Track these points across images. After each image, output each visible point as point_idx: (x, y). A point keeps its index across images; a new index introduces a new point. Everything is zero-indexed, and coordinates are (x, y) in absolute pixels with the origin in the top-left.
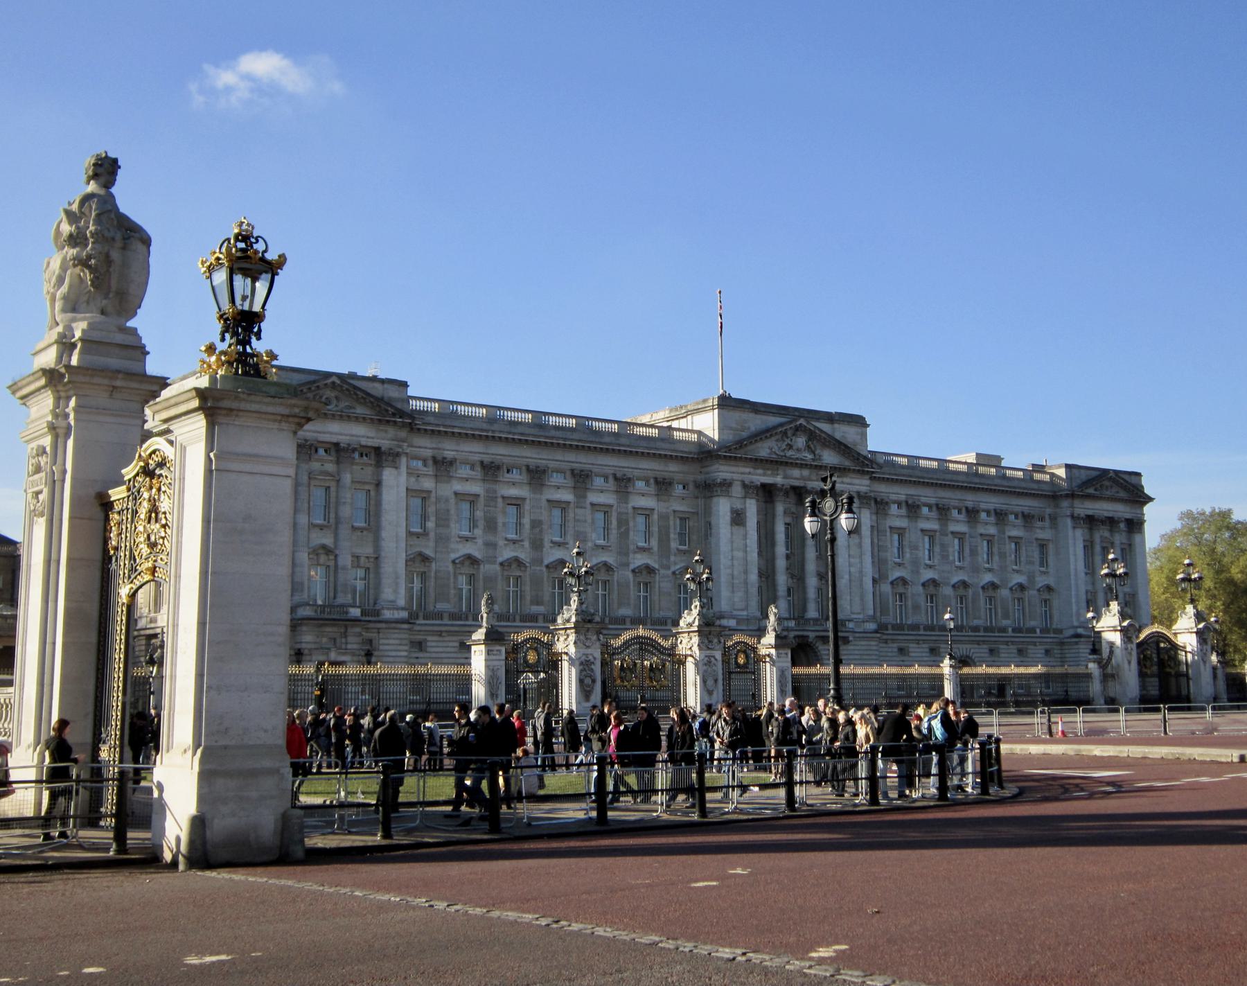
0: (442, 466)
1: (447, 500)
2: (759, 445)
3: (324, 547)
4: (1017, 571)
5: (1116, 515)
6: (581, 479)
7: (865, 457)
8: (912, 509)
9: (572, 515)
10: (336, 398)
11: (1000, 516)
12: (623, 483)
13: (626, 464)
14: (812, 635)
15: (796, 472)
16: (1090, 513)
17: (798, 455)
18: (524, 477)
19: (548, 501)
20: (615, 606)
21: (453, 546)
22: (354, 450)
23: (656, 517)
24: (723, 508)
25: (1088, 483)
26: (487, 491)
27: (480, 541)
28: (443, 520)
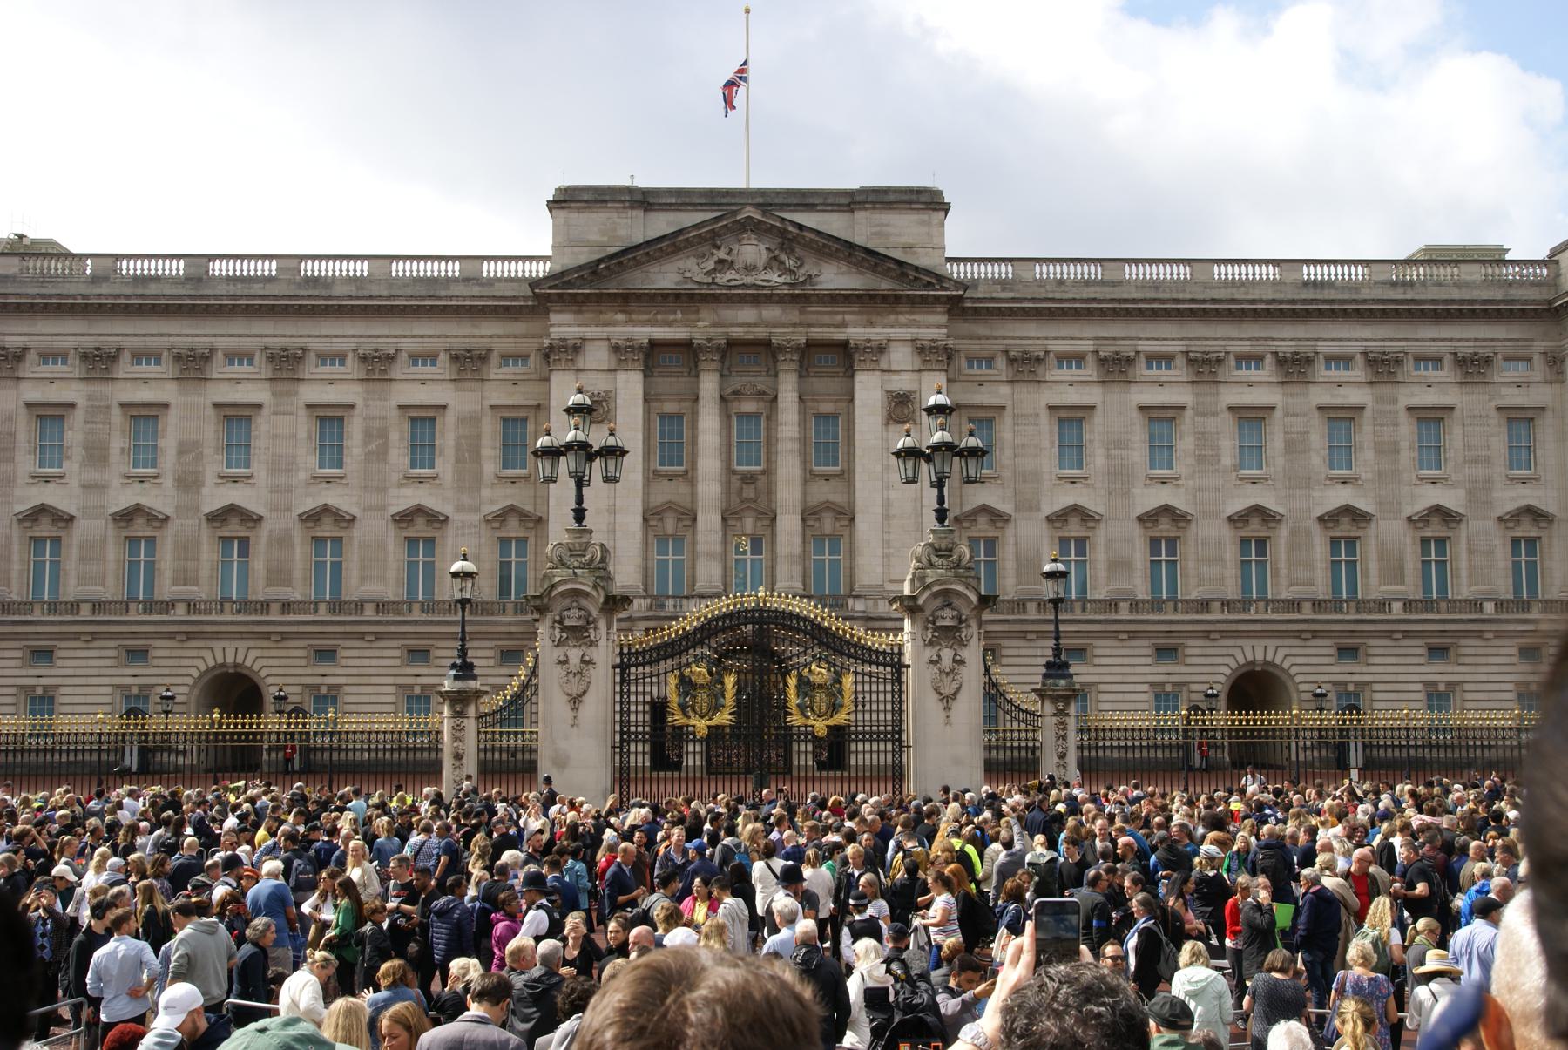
1: (9, 419)
2: (654, 268)
4: (1434, 481)
6: (286, 364)
7: (917, 269)
8: (1116, 367)
9: (264, 428)
11: (1382, 367)
12: (377, 365)
13: (386, 332)
15: (747, 314)
17: (749, 280)
18: (167, 368)
19: (216, 406)
20: (354, 581)
21: (18, 492)
26: (89, 397)
27: (74, 482)
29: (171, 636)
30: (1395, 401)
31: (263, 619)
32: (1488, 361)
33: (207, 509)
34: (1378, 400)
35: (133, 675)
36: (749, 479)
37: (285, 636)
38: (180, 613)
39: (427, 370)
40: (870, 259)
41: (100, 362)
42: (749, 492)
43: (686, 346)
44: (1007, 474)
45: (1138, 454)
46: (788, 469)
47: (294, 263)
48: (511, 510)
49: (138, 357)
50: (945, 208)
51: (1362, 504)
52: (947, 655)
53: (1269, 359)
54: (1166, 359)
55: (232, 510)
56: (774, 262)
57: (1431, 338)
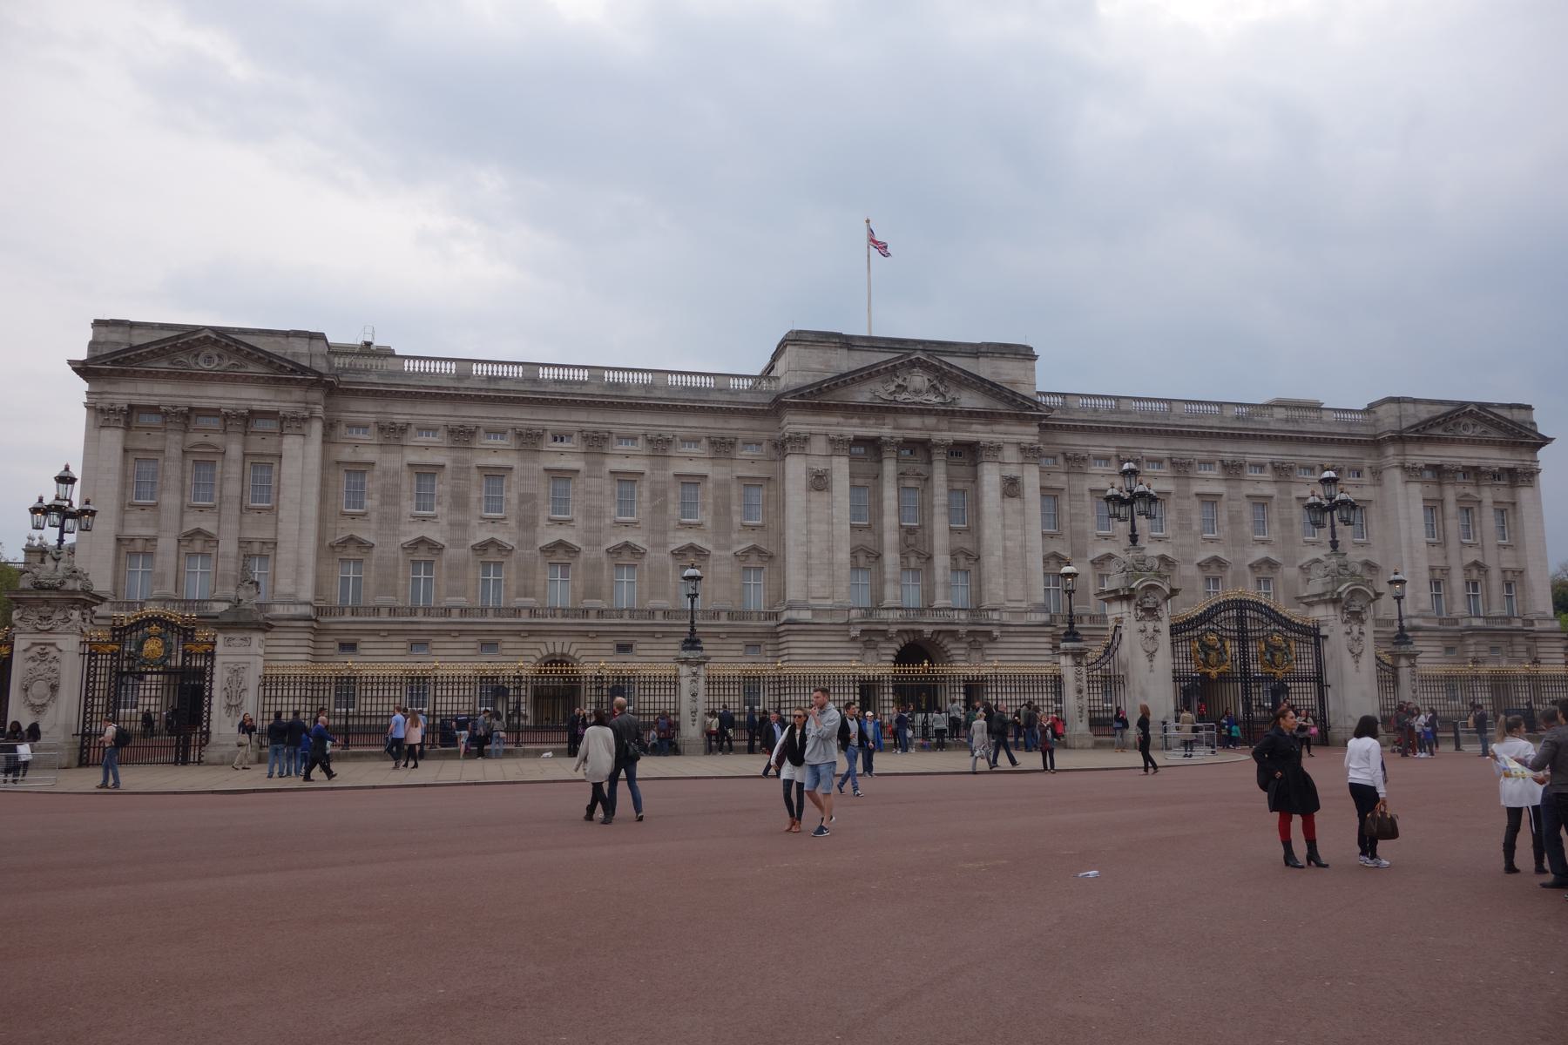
0: (392, 433)
1: (396, 473)
3: (198, 532)
4: (1313, 544)
5: (1483, 464)
6: (596, 442)
7: (1024, 397)
9: (581, 486)
10: (219, 356)
12: (660, 446)
14: (928, 630)
15: (915, 421)
16: (1437, 461)
17: (917, 399)
18: (507, 442)
21: (402, 528)
22: (240, 416)
23: (710, 485)
24: (796, 468)
25: (1433, 422)
26: (454, 461)
27: (444, 522)
28: (390, 497)
29: (517, 633)
30: (1290, 493)
31: (586, 622)
33: (541, 544)
34: (1280, 492)
35: (488, 664)
36: (911, 531)
37: (599, 634)
38: (525, 618)
39: (693, 450)
41: (462, 436)
42: (911, 540)
44: (1066, 532)
46: (940, 525)
47: (599, 372)
48: (755, 549)
49: (489, 432)
50: (1033, 358)
52: (1356, 628)
53: (1218, 464)
54: (1159, 462)
55: (560, 544)
57: (1308, 454)
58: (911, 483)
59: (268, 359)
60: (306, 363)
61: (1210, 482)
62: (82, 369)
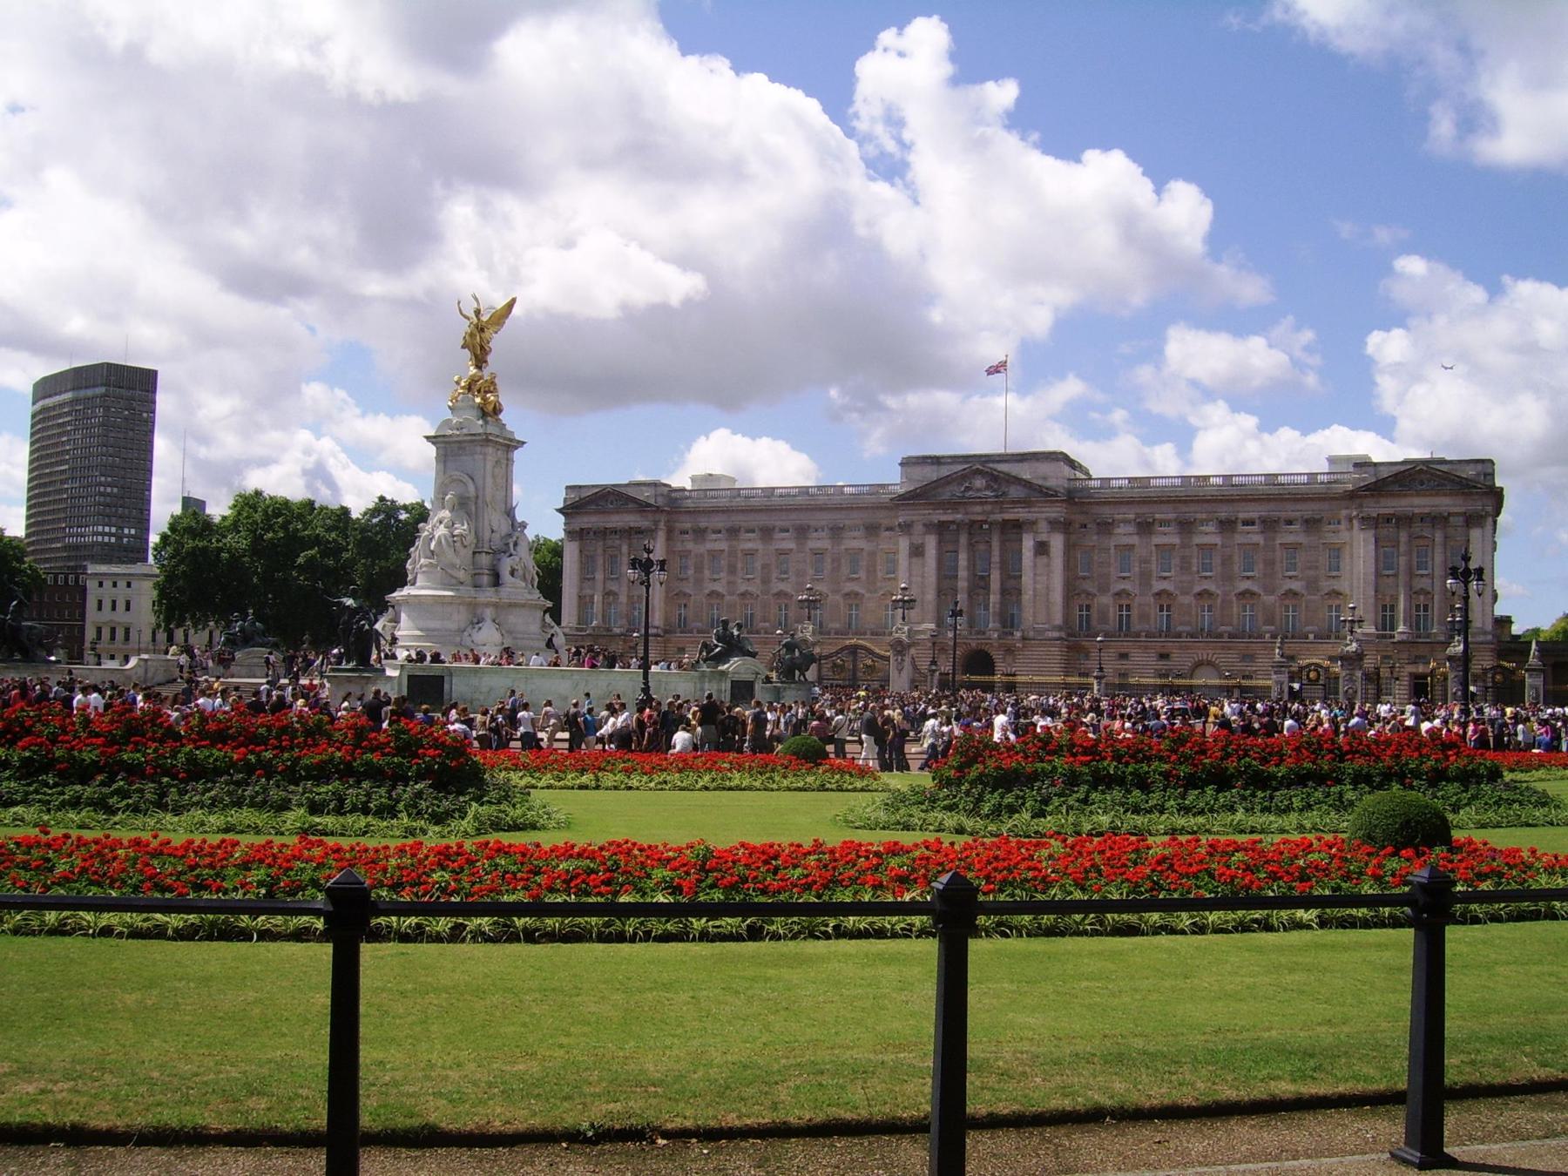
1: (702, 555)
8: (1145, 527)
11: (1269, 525)
12: (836, 532)
15: (978, 509)
16: (1391, 511)
27: (724, 582)
28: (699, 569)
32: (1320, 521)
36: (982, 577)
39: (856, 534)
40: (1027, 484)
41: (733, 532)
43: (953, 522)
45: (1154, 567)
46: (995, 576)
51: (1255, 589)
56: (988, 487)
57: (1290, 511)
58: (982, 547)
59: (634, 500)
60: (652, 501)
61: (1208, 535)
62: (560, 511)
